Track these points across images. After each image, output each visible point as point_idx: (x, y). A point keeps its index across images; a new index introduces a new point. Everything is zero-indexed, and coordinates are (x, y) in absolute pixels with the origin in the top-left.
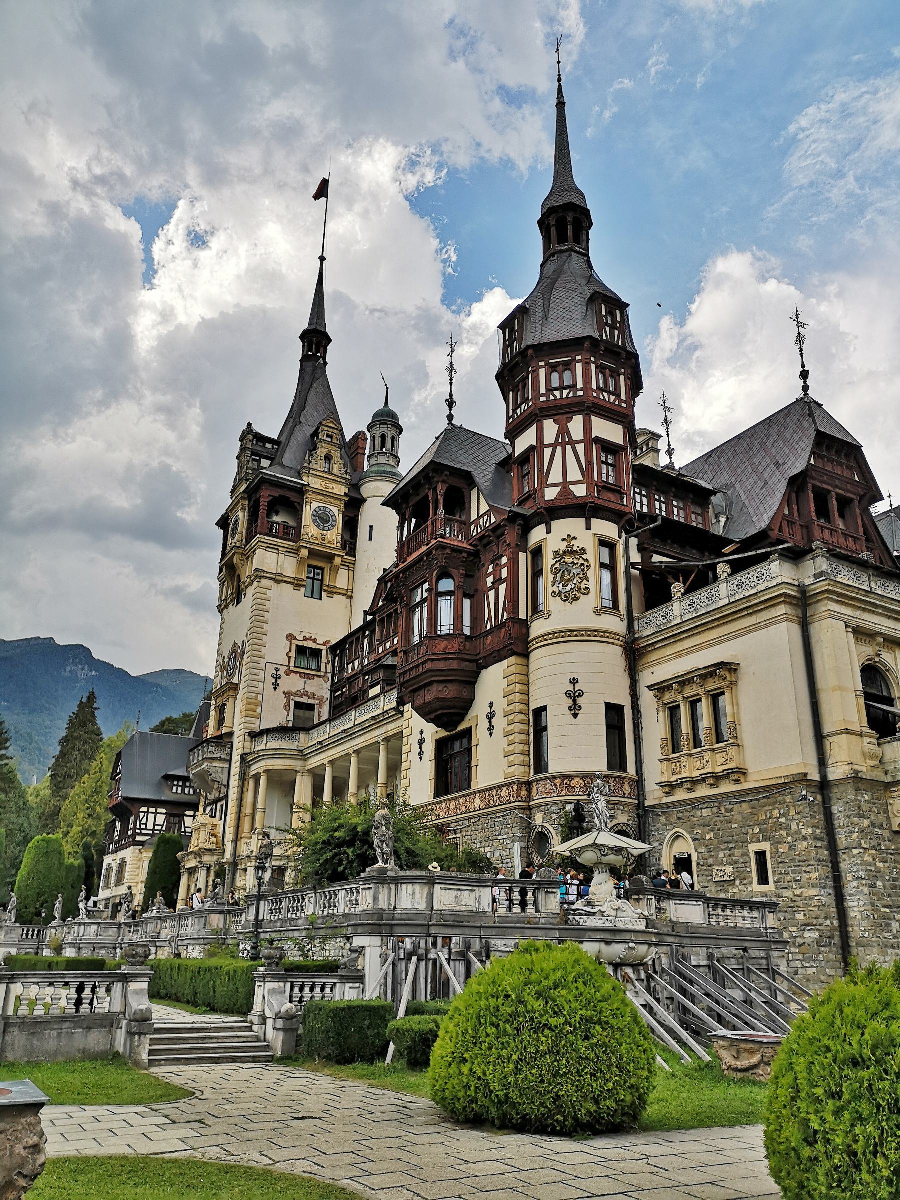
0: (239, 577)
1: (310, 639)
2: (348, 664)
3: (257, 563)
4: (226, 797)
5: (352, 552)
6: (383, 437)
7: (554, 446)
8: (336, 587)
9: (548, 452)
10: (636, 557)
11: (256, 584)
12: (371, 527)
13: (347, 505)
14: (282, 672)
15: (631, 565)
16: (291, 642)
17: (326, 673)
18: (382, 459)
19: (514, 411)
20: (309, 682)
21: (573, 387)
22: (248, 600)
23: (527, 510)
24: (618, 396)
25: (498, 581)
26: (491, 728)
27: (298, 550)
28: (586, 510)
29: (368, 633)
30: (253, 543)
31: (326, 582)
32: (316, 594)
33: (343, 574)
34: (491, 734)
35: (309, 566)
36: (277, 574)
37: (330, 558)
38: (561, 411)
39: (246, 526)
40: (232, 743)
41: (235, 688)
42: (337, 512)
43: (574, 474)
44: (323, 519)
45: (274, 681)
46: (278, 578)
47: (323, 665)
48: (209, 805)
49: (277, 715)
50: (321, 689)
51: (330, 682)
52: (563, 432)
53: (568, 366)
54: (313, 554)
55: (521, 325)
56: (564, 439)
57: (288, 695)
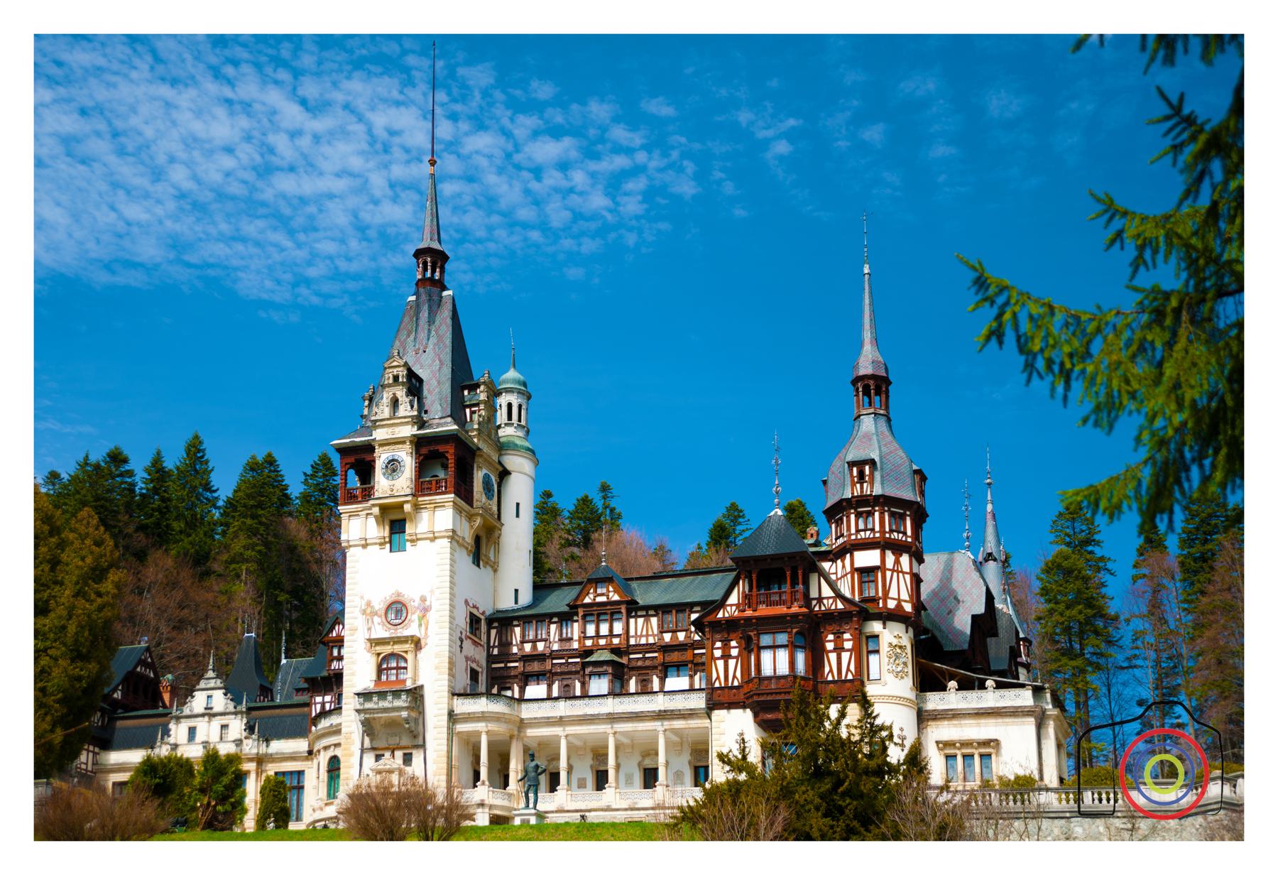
2: (522, 642)
7: (893, 570)
9: (888, 574)
19: (858, 531)
21: (905, 533)
23: (871, 608)
25: (839, 649)
29: (555, 619)
38: (898, 548)
41: (417, 644)
43: (905, 596)
49: (464, 681)
52: (897, 562)
53: (903, 517)
55: (872, 474)
56: (897, 569)
57: (467, 658)
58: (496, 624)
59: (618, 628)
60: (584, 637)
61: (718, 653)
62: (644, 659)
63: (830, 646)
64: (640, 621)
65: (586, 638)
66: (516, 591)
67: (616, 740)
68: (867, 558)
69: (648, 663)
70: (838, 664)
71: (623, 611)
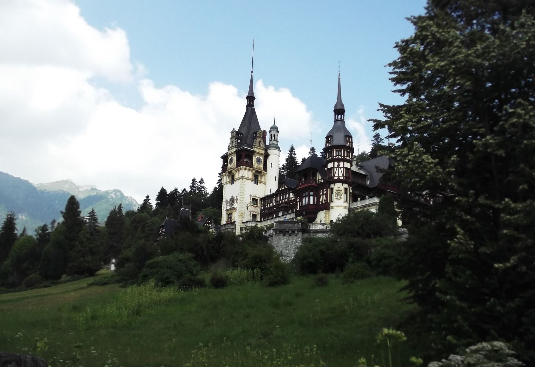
0: (233, 177)
6: (274, 135)
9: (335, 169)
10: (351, 191)
11: (241, 180)
15: (350, 193)
21: (341, 155)
22: (237, 183)
24: (349, 157)
28: (342, 182)
31: (259, 179)
33: (264, 177)
37: (260, 173)
38: (339, 161)
42: (262, 158)
43: (341, 174)
44: (259, 161)
49: (248, 218)
52: (339, 165)
53: (341, 151)
54: (257, 171)
56: (339, 167)
57: (250, 212)
61: (298, 200)
63: (321, 193)
65: (280, 200)
68: (330, 165)
70: (322, 199)
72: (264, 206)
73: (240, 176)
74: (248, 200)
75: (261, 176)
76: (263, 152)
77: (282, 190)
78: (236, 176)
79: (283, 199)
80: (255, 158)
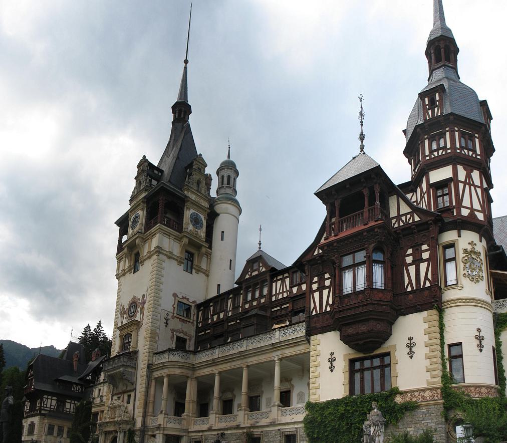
0: (137, 255)
1: (185, 298)
2: (212, 316)
3: (155, 242)
4: (135, 389)
5: (210, 247)
6: (229, 177)
8: (200, 267)
11: (155, 257)
12: (223, 232)
13: (208, 215)
14: (170, 317)
16: (175, 298)
17: (193, 321)
18: (229, 191)
20: (184, 324)
22: (147, 268)
26: (411, 354)
27: (181, 238)
29: (231, 296)
30: (153, 230)
31: (195, 262)
32: (189, 270)
33: (205, 259)
34: (411, 357)
35: (187, 251)
36: (171, 253)
37: (199, 247)
39: (144, 220)
40: (137, 358)
41: (138, 324)
42: (203, 217)
44: (196, 221)
45: (165, 321)
46: (169, 254)
47: (192, 316)
48: (116, 394)
49: (167, 342)
50: (190, 330)
51: (195, 326)
54: (192, 243)
57: (173, 331)
58: (202, 308)
59: (265, 291)
60: (245, 301)
62: (281, 309)
64: (279, 283)
66: (219, 285)
67: (249, 375)
69: (283, 312)
71: (268, 278)
72: (205, 319)
73: (153, 249)
74: (168, 304)
75: (201, 256)
76: (206, 205)
77: (252, 278)
78: (145, 253)
79: (253, 299)
80: (188, 214)
